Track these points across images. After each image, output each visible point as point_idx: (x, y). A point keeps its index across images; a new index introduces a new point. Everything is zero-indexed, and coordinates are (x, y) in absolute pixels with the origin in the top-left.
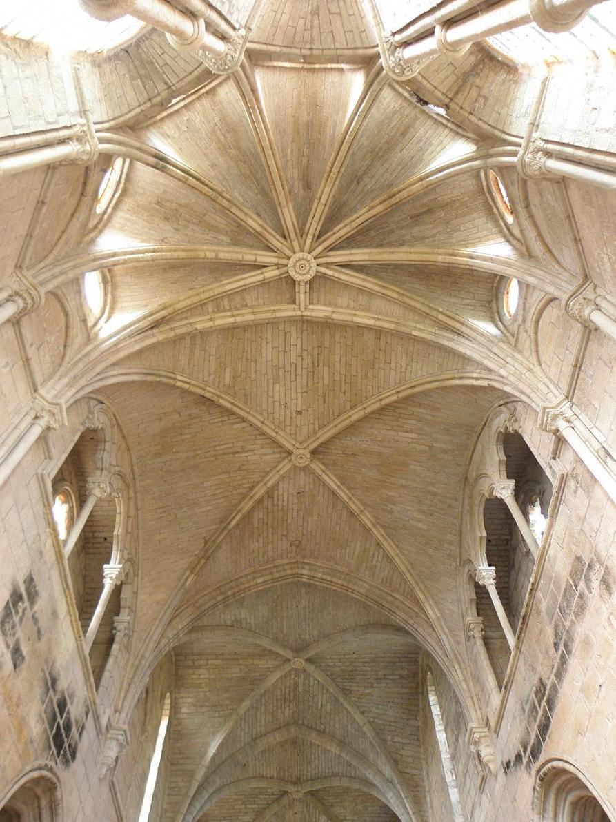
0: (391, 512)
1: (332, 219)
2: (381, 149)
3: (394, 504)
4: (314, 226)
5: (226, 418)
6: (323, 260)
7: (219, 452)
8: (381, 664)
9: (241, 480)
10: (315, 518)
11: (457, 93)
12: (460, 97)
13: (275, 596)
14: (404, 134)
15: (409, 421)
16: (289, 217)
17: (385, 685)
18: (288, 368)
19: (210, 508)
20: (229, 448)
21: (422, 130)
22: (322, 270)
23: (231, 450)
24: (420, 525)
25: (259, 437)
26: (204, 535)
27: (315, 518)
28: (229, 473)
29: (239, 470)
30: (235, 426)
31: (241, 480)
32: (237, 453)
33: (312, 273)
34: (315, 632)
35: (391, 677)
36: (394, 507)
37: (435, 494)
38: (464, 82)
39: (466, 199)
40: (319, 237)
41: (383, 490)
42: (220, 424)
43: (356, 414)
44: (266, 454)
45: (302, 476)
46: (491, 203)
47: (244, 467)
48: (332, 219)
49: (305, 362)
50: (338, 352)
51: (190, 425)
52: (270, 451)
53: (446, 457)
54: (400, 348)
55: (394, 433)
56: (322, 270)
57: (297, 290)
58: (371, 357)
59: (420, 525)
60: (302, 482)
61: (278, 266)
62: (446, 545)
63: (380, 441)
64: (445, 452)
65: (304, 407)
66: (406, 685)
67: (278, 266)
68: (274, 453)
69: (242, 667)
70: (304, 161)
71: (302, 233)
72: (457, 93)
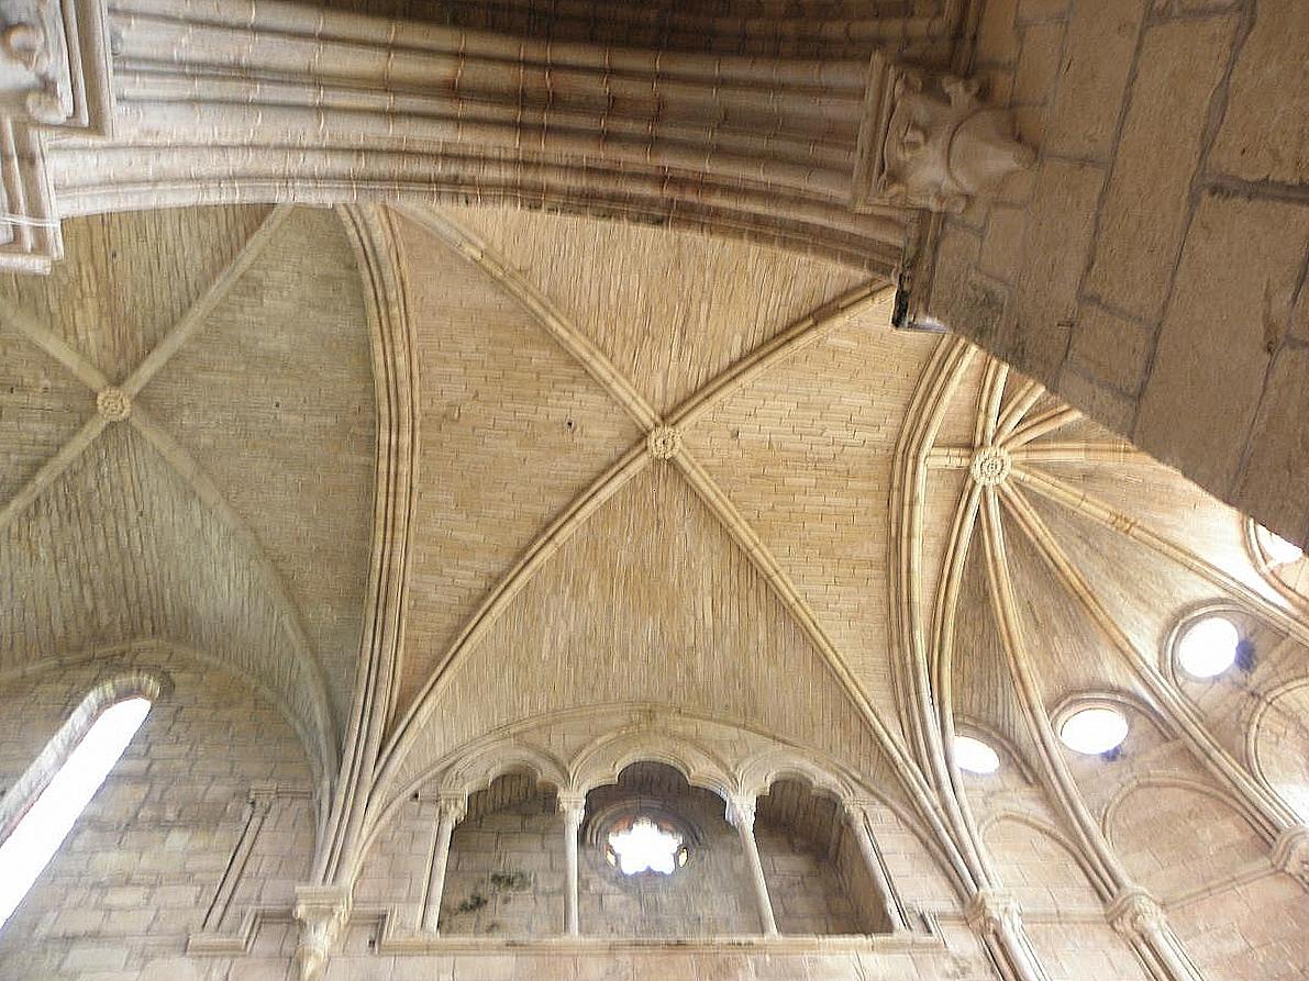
0: (555, 591)
1: (1038, 502)
2: (1120, 568)
3: (572, 595)
4: (1041, 483)
5: (760, 325)
6: (990, 493)
7: (694, 309)
8: (118, 570)
9: (624, 333)
10: (516, 452)
11: (1278, 710)
12: (1271, 713)
13: (315, 367)
14: (1140, 598)
15: (735, 611)
16: (1058, 456)
17: (65, 584)
18: (818, 423)
19: (586, 278)
20: (698, 320)
21: (1147, 622)
22: (978, 490)
23: (691, 324)
24: (546, 647)
25: (703, 371)
26: (536, 270)
27: (516, 452)
28: (645, 314)
29: (646, 332)
30: (738, 338)
31: (624, 333)
32: (683, 334)
33: (981, 481)
34: (206, 440)
35: (87, 593)
36: (567, 595)
37: (607, 662)
38: (1289, 719)
39: (1056, 671)
40: (1019, 485)
41: (594, 576)
42: (752, 315)
43: (744, 532)
44: (665, 377)
45: (607, 434)
46: (1062, 705)
47: (648, 341)
48: (1038, 502)
49: (823, 449)
50: (842, 501)
51: (773, 273)
52: (673, 383)
53: (680, 673)
54: (864, 600)
55: (707, 586)
56: (978, 490)
57: (952, 452)
58: (839, 552)
59: (546, 647)
60: (594, 431)
61: (999, 431)
62: (527, 698)
63: (689, 564)
64: (690, 671)
65: (743, 443)
66: (72, 628)
67: (999, 431)
68: (665, 392)
69: (72, 269)
70: (1122, 476)
71: (1030, 466)
72: (1278, 710)
